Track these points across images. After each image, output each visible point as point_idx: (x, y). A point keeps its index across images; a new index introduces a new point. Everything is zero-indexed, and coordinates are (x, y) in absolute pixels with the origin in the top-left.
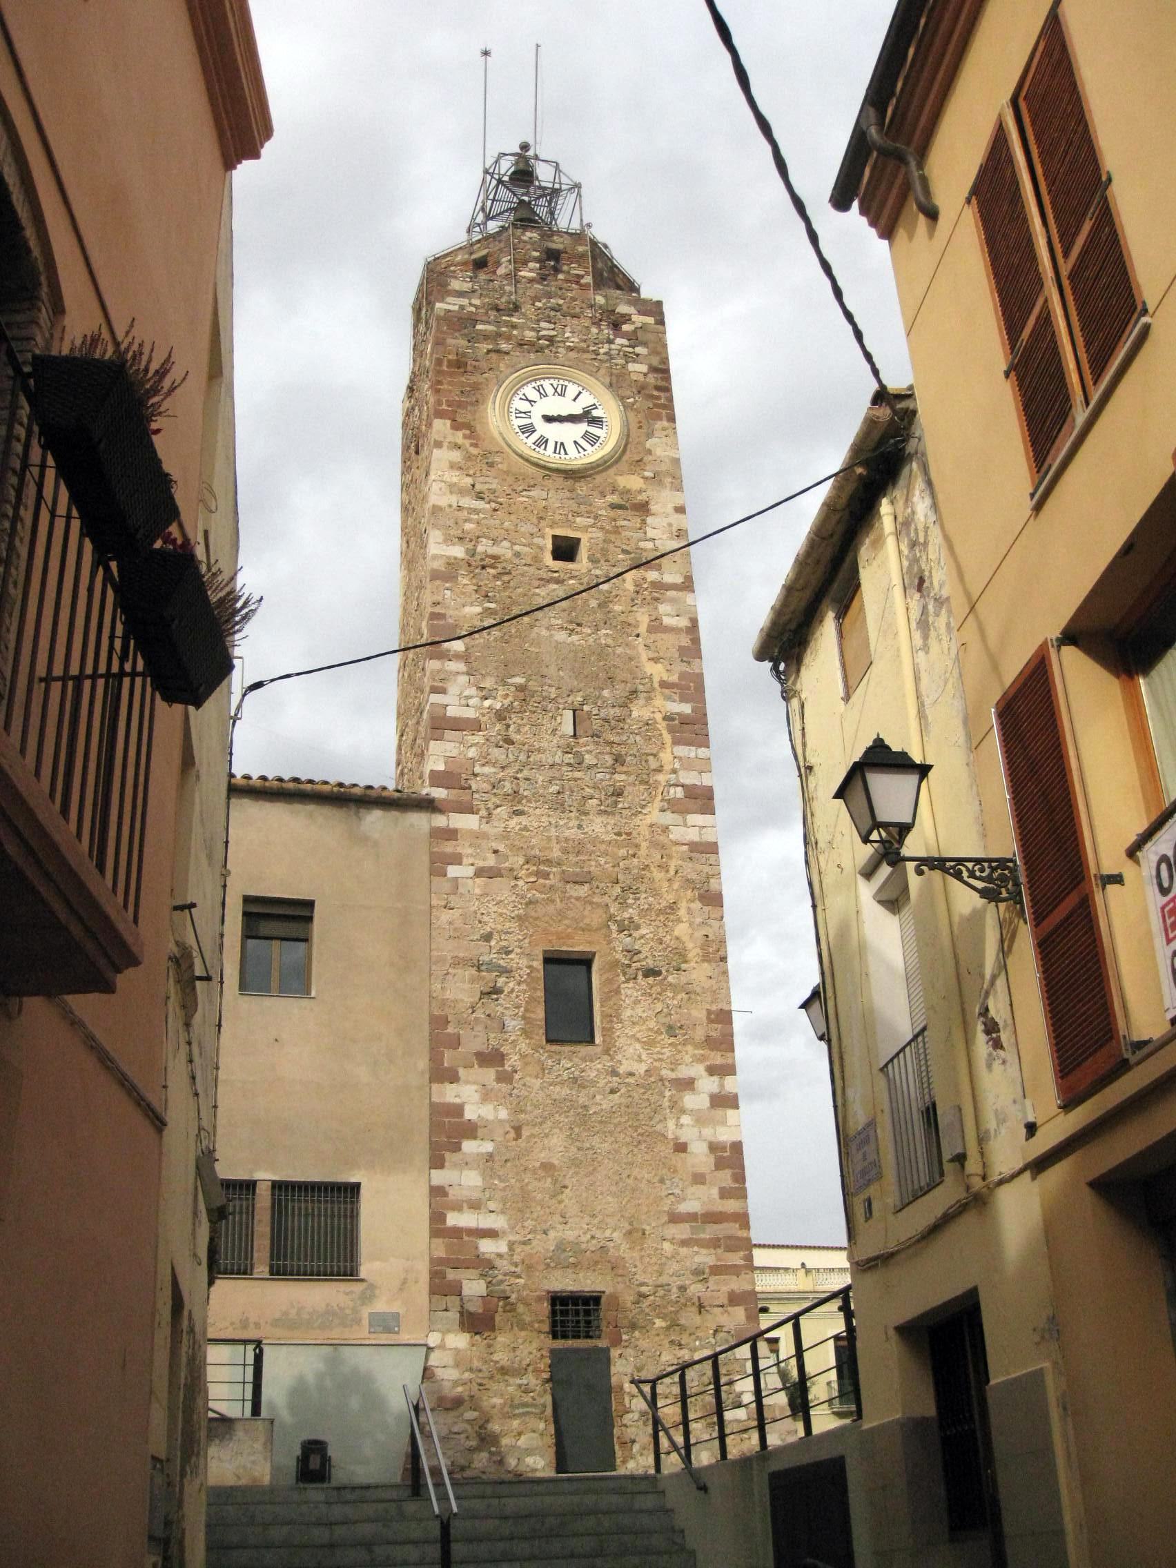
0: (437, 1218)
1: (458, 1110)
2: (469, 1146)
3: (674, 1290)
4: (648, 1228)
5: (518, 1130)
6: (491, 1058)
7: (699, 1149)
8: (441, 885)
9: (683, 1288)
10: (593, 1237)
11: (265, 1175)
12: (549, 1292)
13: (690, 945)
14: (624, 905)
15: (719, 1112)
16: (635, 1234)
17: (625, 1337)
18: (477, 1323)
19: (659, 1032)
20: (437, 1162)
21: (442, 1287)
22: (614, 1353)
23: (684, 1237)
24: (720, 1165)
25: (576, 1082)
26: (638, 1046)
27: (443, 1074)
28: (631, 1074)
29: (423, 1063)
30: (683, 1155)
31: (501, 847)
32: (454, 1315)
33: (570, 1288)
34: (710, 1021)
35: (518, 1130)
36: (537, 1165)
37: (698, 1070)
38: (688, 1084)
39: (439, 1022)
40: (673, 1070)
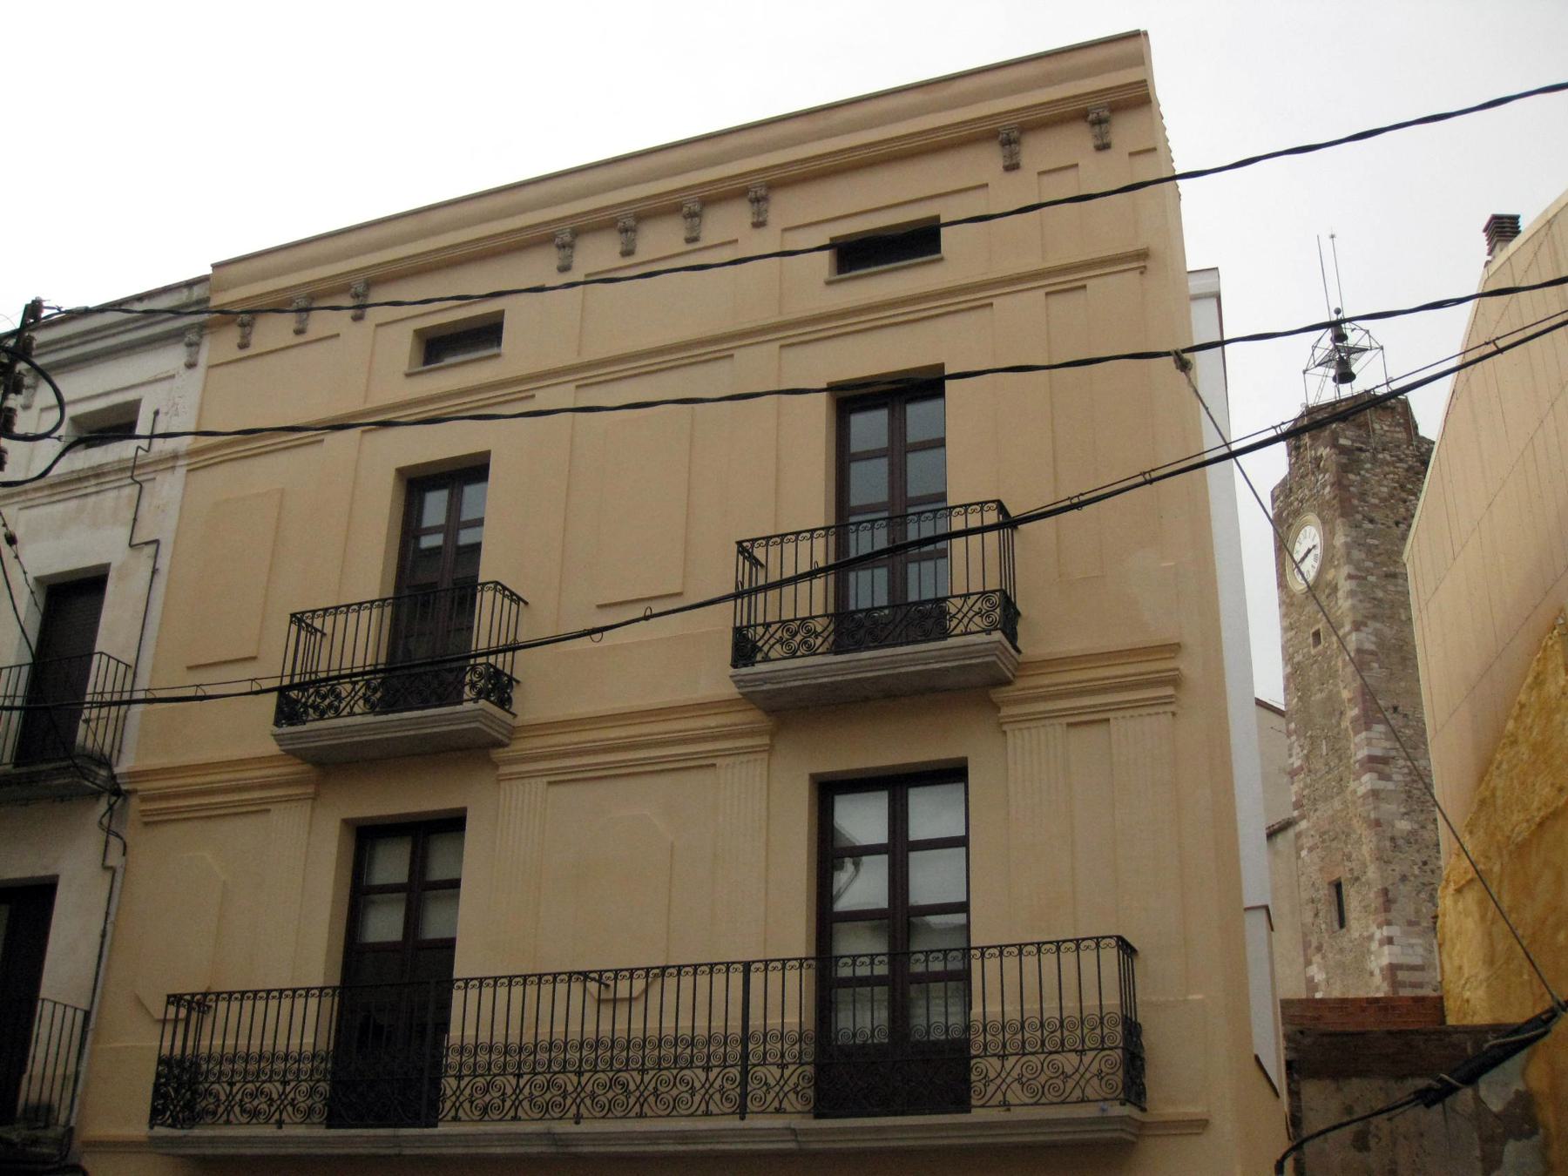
1: (1312, 978)
6: (1319, 949)
7: (1377, 972)
24: (1384, 978)
25: (1341, 950)
27: (1308, 963)
29: (1302, 960)
37: (1373, 928)
38: (1371, 938)
39: (1305, 935)
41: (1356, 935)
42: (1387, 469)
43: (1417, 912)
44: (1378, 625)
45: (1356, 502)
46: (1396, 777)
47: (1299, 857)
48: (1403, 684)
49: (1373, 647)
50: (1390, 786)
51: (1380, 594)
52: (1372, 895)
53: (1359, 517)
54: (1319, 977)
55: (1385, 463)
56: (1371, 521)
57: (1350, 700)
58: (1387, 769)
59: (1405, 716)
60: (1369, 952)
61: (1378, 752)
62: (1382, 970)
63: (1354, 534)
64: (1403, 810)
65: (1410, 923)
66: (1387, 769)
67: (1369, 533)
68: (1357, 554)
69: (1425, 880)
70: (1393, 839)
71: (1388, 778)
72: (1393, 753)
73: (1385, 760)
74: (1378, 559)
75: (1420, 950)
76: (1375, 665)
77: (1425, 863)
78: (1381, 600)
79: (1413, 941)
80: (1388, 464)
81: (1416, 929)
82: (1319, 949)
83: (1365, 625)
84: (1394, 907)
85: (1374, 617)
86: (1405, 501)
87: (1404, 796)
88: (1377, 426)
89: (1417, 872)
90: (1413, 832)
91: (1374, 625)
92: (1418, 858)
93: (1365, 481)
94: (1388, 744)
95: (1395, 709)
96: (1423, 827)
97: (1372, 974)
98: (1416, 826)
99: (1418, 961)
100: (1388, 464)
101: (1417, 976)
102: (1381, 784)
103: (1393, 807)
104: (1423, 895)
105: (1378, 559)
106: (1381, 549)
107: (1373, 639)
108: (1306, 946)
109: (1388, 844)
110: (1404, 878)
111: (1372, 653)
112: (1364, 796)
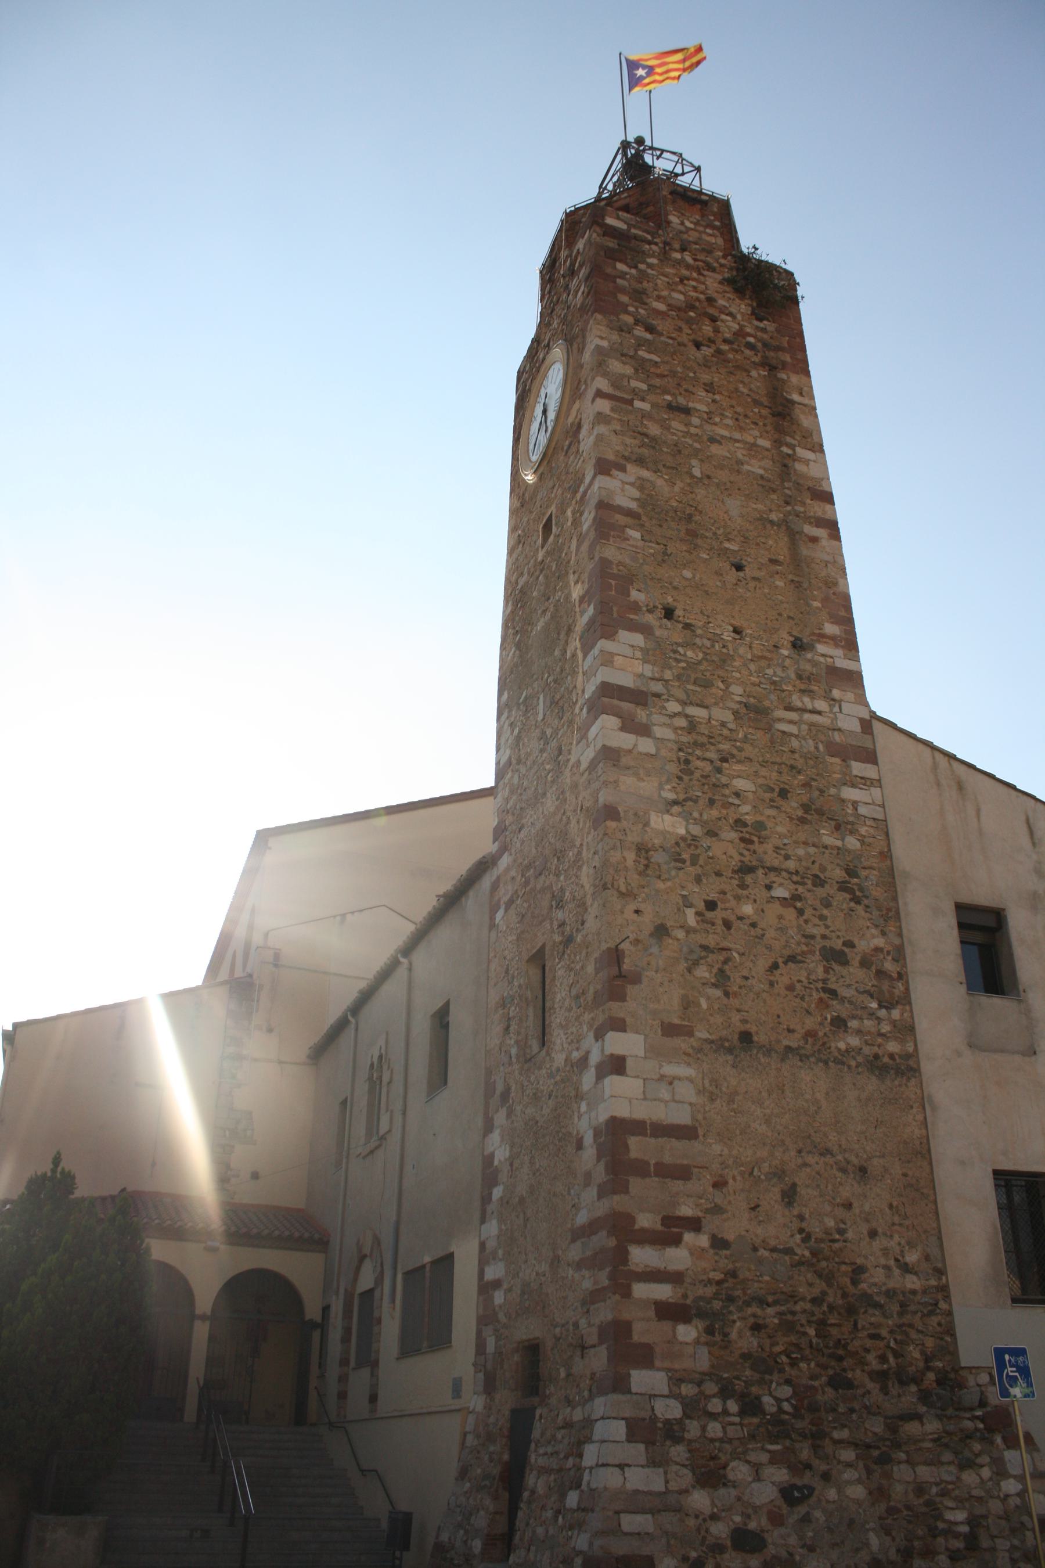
0: (481, 1273)
1: (492, 1156)
2: (497, 1192)
3: (571, 1328)
4: (560, 1252)
5: (511, 1165)
7: (588, 1139)
8: (493, 934)
9: (576, 1325)
10: (537, 1274)
11: (427, 1259)
12: (519, 1343)
13: (587, 886)
14: (557, 875)
15: (600, 1086)
16: (555, 1262)
17: (548, 1392)
18: (490, 1386)
19: (570, 1010)
20: (483, 1220)
21: (480, 1347)
22: (538, 1412)
23: (577, 1258)
26: (561, 1032)
27: (488, 1127)
28: (558, 1070)
29: (480, 1122)
30: (580, 1152)
31: (513, 873)
32: (481, 1375)
33: (524, 1337)
34: (597, 971)
35: (511, 1165)
36: (517, 1199)
39: (489, 1072)
40: (578, 1049)
41: (559, 1059)
42: (685, 272)
43: (687, 1004)
44: (646, 474)
45: (624, 299)
46: (659, 732)
47: (492, 926)
48: (687, 574)
49: (633, 505)
50: (646, 745)
51: (654, 430)
52: (590, 969)
53: (630, 320)
54: (501, 1154)
55: (681, 262)
56: (650, 329)
57: (582, 599)
58: (641, 715)
59: (687, 626)
60: (579, 1097)
61: (626, 680)
62: (597, 1134)
63: (615, 337)
64: (671, 796)
65: (670, 1030)
66: (641, 715)
67: (640, 343)
68: (616, 366)
69: (711, 941)
70: (642, 849)
71: (643, 730)
72: (657, 687)
73: (639, 697)
74: (657, 382)
75: (687, 1092)
76: (636, 535)
77: (711, 905)
78: (654, 439)
79: (669, 1070)
80: (688, 267)
81: (681, 1043)
82: (505, 1096)
83: (623, 469)
84: (631, 990)
85: (640, 461)
86: (714, 320)
87: (673, 768)
88: (674, 219)
89: (691, 920)
90: (691, 841)
91: (634, 472)
92: (699, 895)
93: (643, 276)
94: (648, 670)
95: (669, 613)
96: (712, 834)
97: (580, 1146)
98: (696, 830)
99: (681, 1116)
100: (688, 267)
101: (673, 1151)
102: (625, 740)
103: (648, 787)
104: (702, 972)
105: (657, 382)
106: (663, 369)
107: (636, 494)
108: (489, 1090)
109: (631, 856)
110: (661, 931)
111: (629, 513)
112: (592, 766)
